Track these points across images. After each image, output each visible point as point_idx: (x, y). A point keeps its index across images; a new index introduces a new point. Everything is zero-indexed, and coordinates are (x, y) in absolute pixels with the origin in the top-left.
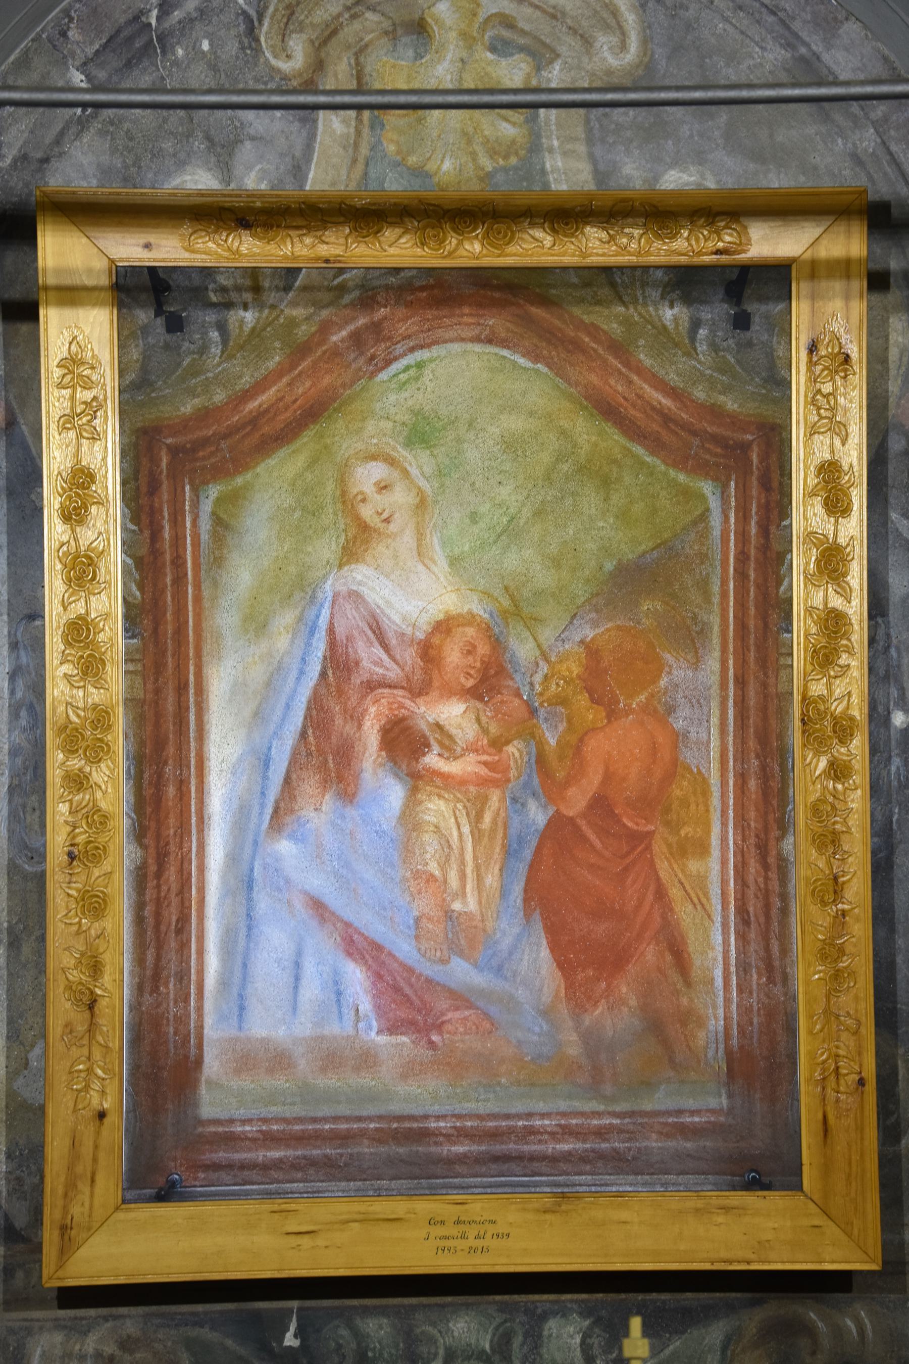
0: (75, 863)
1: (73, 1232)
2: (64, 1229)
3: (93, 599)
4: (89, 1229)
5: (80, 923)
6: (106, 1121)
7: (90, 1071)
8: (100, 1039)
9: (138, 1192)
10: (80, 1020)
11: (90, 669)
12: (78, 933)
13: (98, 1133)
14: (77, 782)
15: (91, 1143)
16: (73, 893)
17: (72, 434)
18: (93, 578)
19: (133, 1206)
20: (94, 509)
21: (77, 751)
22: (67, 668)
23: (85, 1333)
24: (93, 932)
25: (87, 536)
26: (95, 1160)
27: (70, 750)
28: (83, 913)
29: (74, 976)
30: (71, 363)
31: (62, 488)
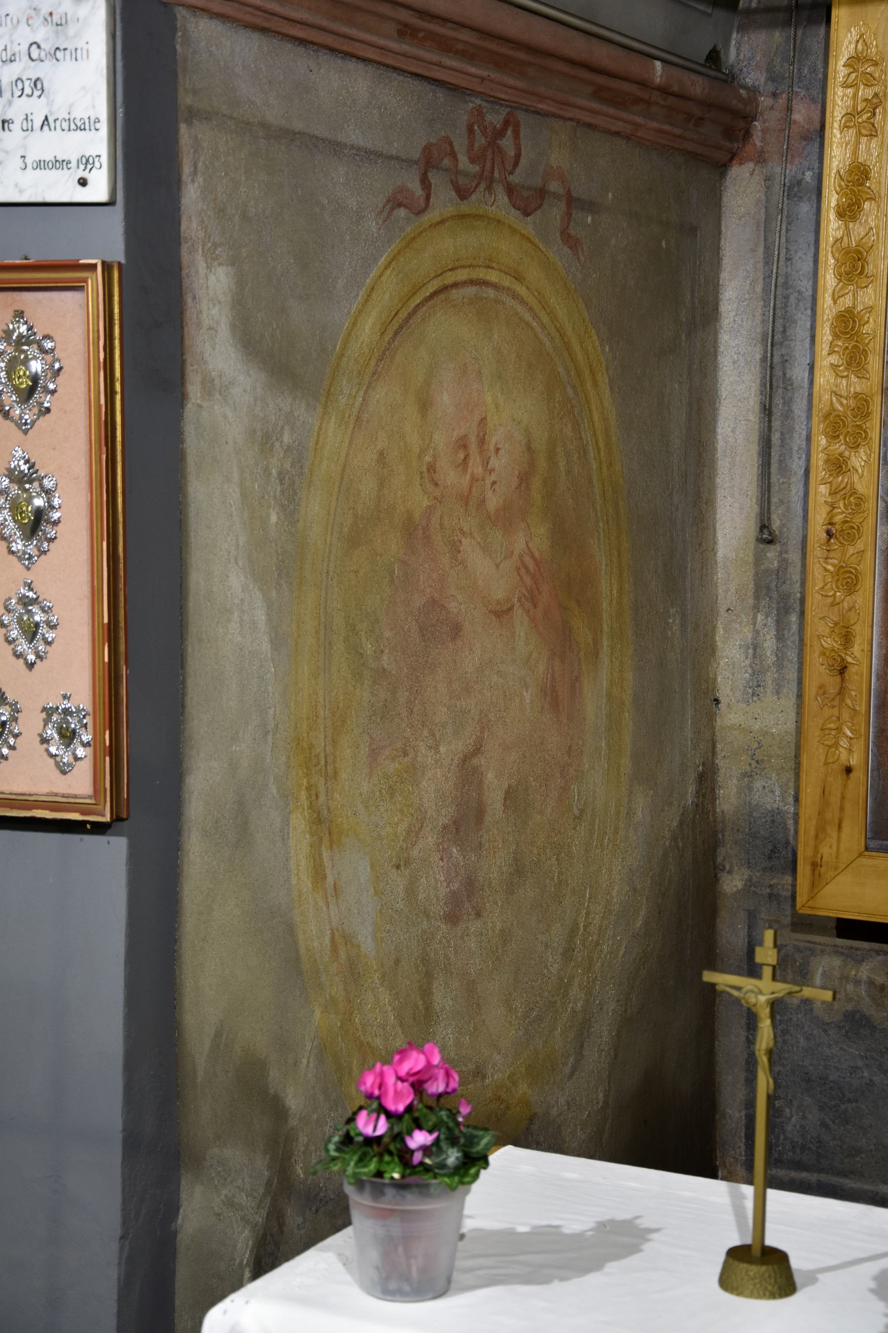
0: (832, 541)
1: (823, 870)
2: (815, 865)
3: (861, 293)
4: (836, 868)
5: (834, 595)
6: (851, 775)
7: (839, 729)
8: (849, 702)
9: (880, 842)
10: (833, 683)
11: (855, 360)
12: (833, 605)
13: (845, 786)
14: (838, 465)
15: (839, 795)
16: (830, 567)
17: (852, 132)
18: (862, 273)
19: (874, 854)
20: (867, 205)
21: (838, 436)
22: (834, 359)
23: (860, 962)
24: (846, 604)
25: (858, 230)
26: (842, 809)
27: (833, 436)
28: (838, 587)
29: (829, 643)
30: (854, 61)
31: (840, 186)
